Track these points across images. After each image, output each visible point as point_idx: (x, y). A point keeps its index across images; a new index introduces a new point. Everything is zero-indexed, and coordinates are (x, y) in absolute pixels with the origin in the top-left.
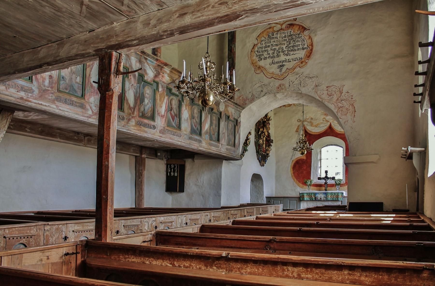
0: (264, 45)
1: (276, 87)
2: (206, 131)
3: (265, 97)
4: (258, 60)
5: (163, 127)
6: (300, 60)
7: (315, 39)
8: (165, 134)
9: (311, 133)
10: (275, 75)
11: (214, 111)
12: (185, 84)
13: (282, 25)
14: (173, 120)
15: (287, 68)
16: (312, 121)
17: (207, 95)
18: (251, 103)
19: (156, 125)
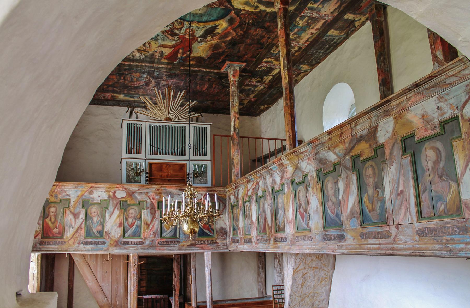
2: (351, 211)
19: (287, 235)
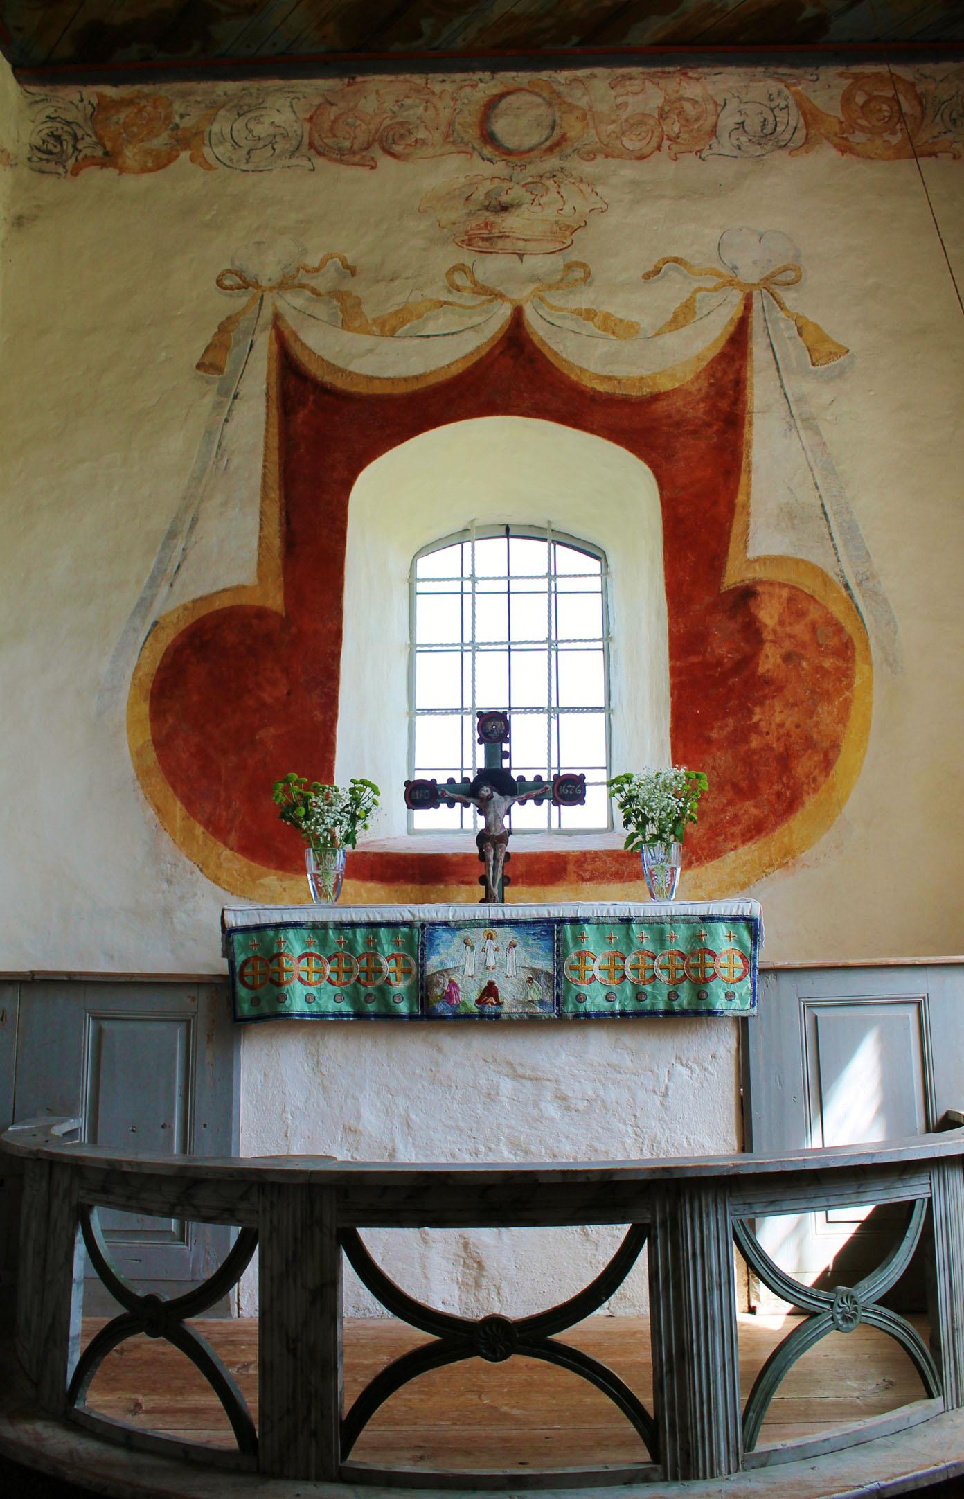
9: (340, 383)
16: (349, 285)
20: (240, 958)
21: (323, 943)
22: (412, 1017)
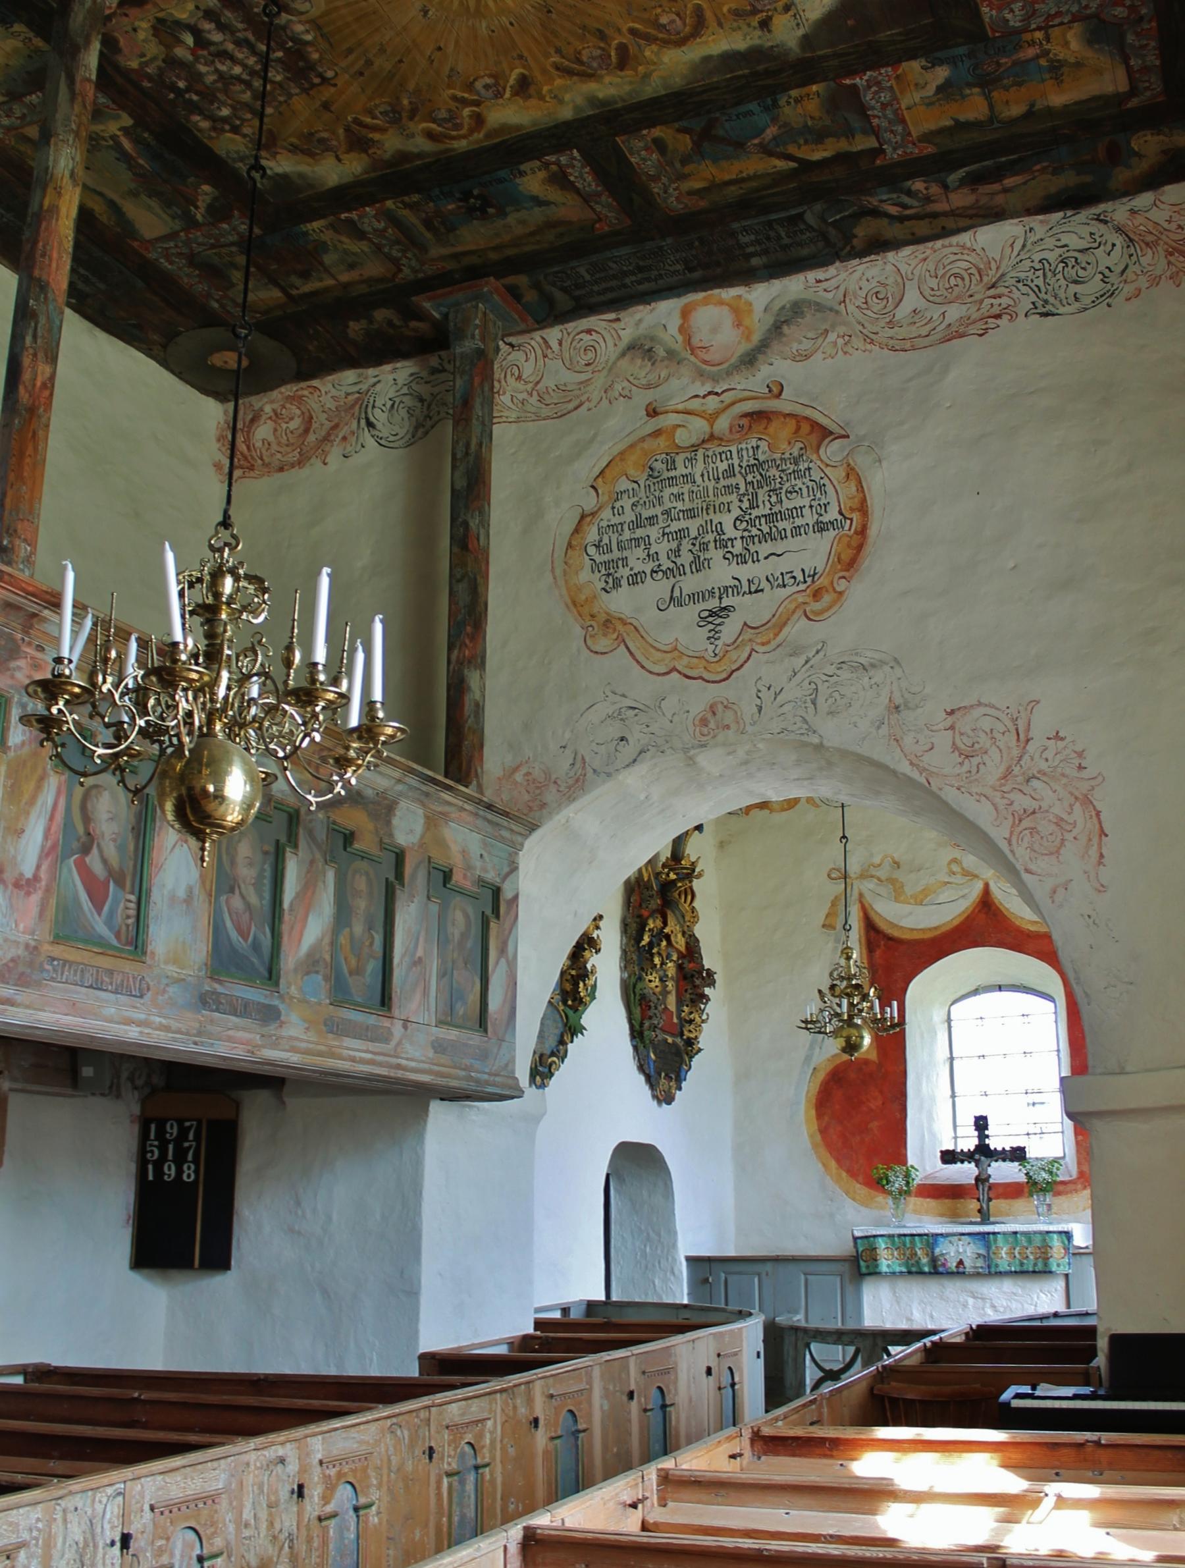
0: (629, 516)
1: (691, 715)
2: (310, 954)
3: (642, 768)
4: (604, 589)
5: (27, 946)
6: (809, 580)
7: (878, 482)
8: (38, 984)
9: (896, 933)
10: (685, 660)
11: (356, 846)
12: (61, 703)
13: (712, 418)
14: (98, 902)
15: (745, 624)
16: (896, 874)
17: (208, 765)
18: (571, 799)
20: (861, 1249)
21: (893, 1243)
22: (930, 1273)
